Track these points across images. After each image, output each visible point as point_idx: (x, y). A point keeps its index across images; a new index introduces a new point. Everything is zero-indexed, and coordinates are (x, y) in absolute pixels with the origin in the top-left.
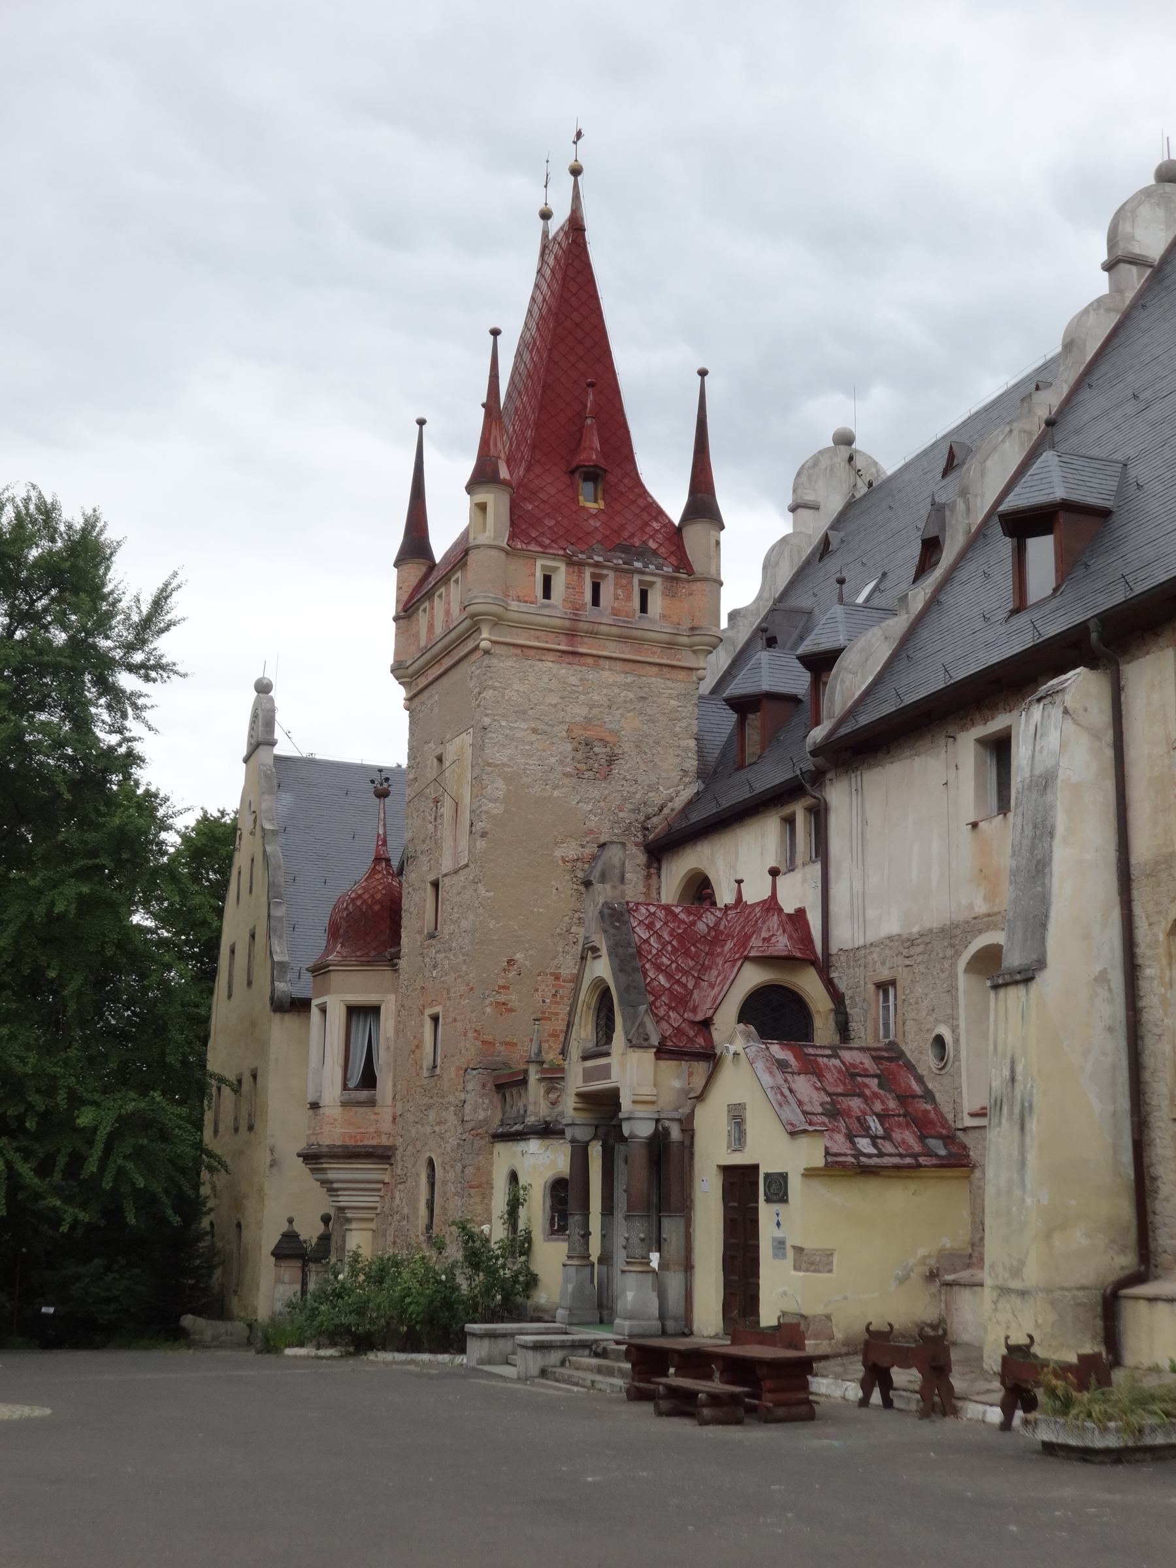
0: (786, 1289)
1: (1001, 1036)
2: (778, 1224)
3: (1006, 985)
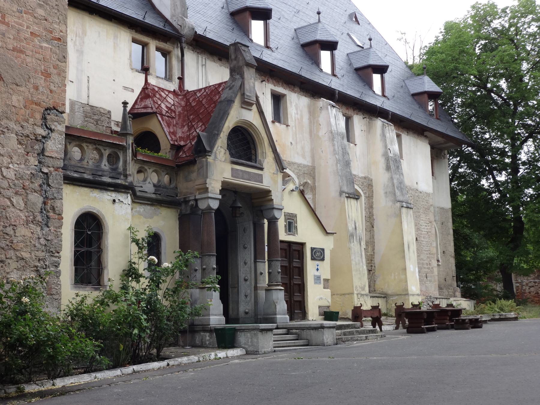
0: (322, 296)
1: (350, 214)
2: (318, 270)
3: (350, 198)
